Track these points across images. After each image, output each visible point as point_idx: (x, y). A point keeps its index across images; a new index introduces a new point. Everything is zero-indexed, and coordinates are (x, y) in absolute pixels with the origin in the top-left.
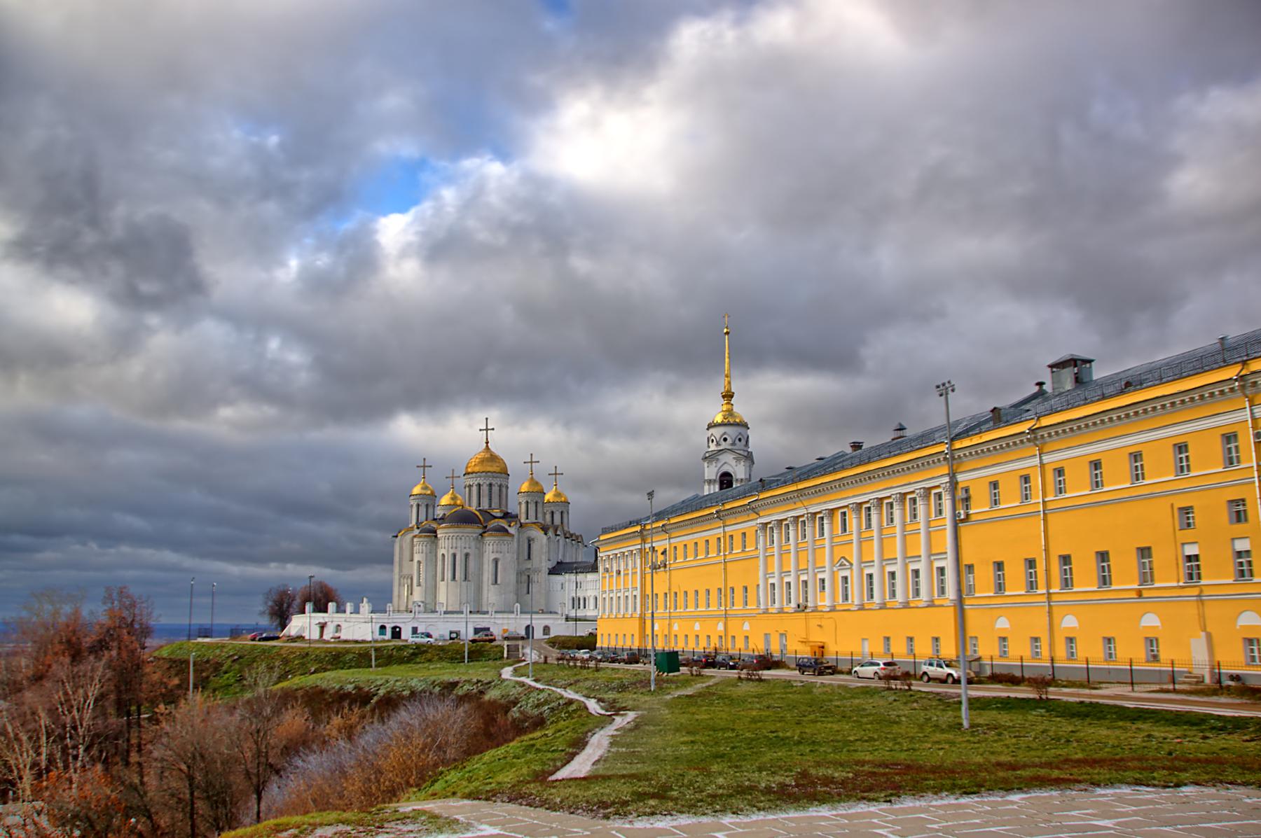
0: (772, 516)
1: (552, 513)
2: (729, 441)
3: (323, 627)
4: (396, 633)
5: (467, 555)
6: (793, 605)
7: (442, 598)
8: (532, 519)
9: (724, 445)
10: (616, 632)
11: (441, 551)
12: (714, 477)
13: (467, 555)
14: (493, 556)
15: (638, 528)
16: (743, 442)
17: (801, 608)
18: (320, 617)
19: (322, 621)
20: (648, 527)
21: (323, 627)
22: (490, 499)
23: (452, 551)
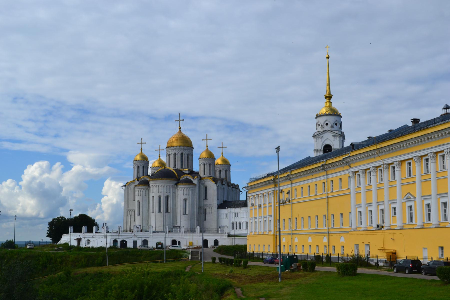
0: (360, 166)
1: (220, 171)
2: (330, 125)
3: (79, 240)
4: (124, 243)
5: (167, 198)
6: (374, 225)
7: (153, 223)
8: (207, 174)
9: (327, 128)
10: (259, 243)
11: (152, 195)
12: (320, 148)
13: (167, 198)
14: (183, 197)
15: (272, 178)
16: (338, 125)
17: (380, 228)
18: (77, 235)
19: (79, 237)
20: (277, 177)
21: (79, 240)
22: (182, 163)
23: (158, 195)
